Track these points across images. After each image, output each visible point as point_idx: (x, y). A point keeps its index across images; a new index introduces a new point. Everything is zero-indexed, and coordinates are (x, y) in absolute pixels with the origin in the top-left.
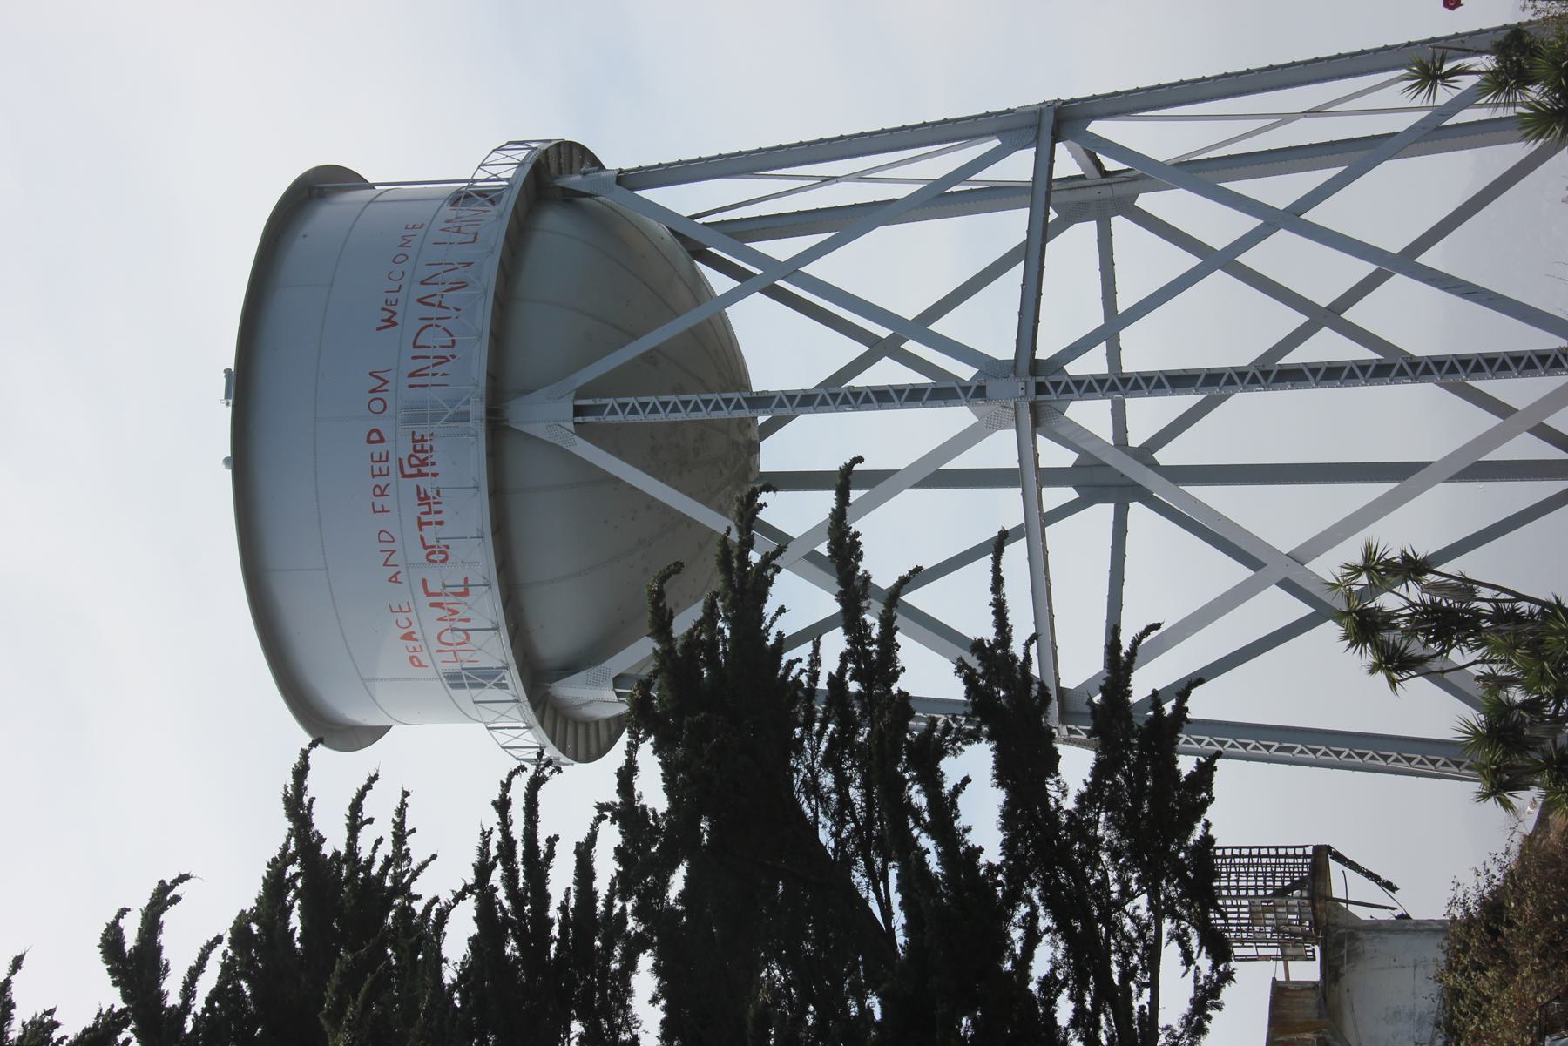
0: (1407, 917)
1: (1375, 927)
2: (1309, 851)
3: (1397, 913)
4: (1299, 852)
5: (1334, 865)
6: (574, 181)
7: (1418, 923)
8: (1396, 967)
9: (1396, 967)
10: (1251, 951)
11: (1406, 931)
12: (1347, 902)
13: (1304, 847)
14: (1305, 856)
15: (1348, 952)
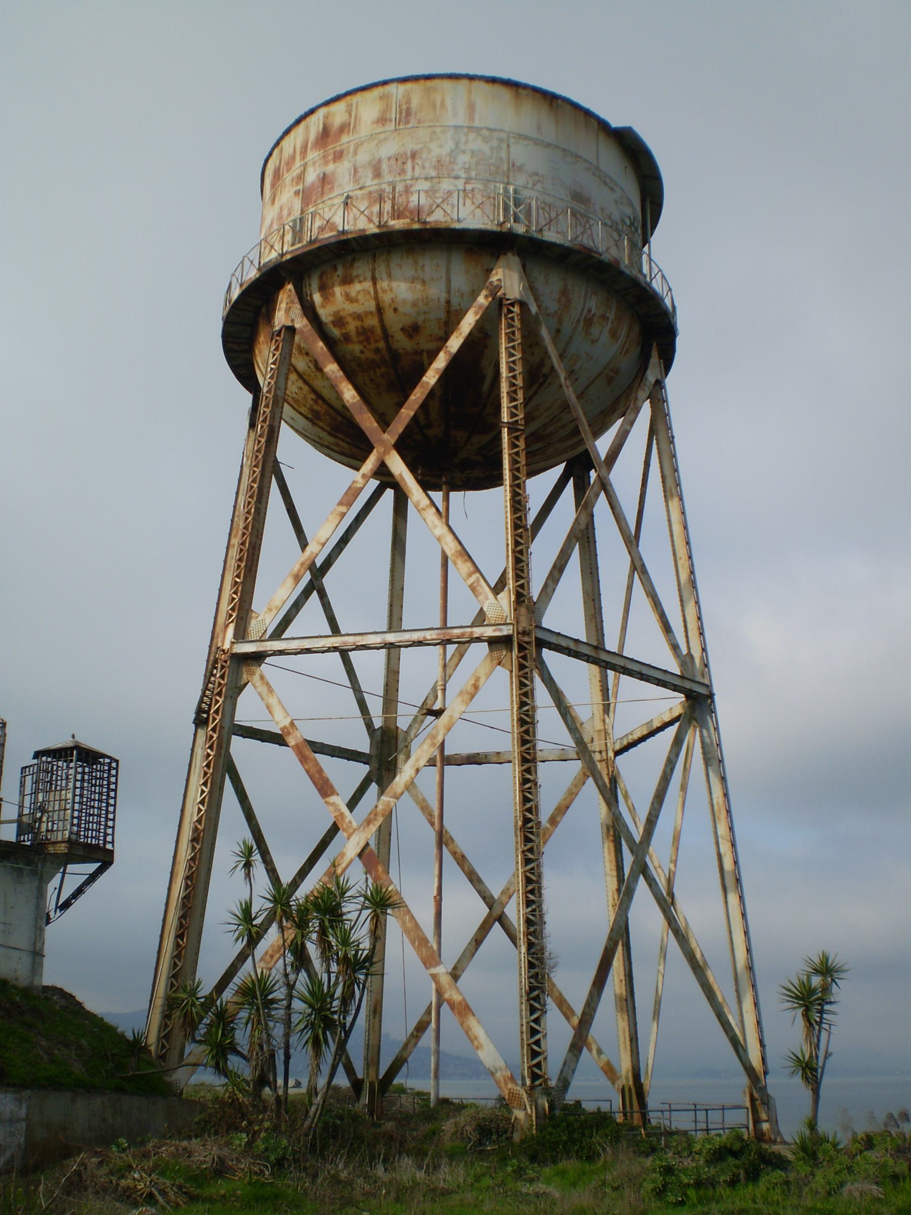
0: (48, 923)
1: (41, 894)
2: (109, 846)
3: (52, 914)
4: (109, 838)
5: (92, 867)
6: (655, 359)
7: (42, 930)
8: (5, 908)
9: (5, 908)
10: (28, 790)
11: (37, 919)
12: (64, 873)
13: (112, 842)
14: (105, 842)
15: (21, 868)
